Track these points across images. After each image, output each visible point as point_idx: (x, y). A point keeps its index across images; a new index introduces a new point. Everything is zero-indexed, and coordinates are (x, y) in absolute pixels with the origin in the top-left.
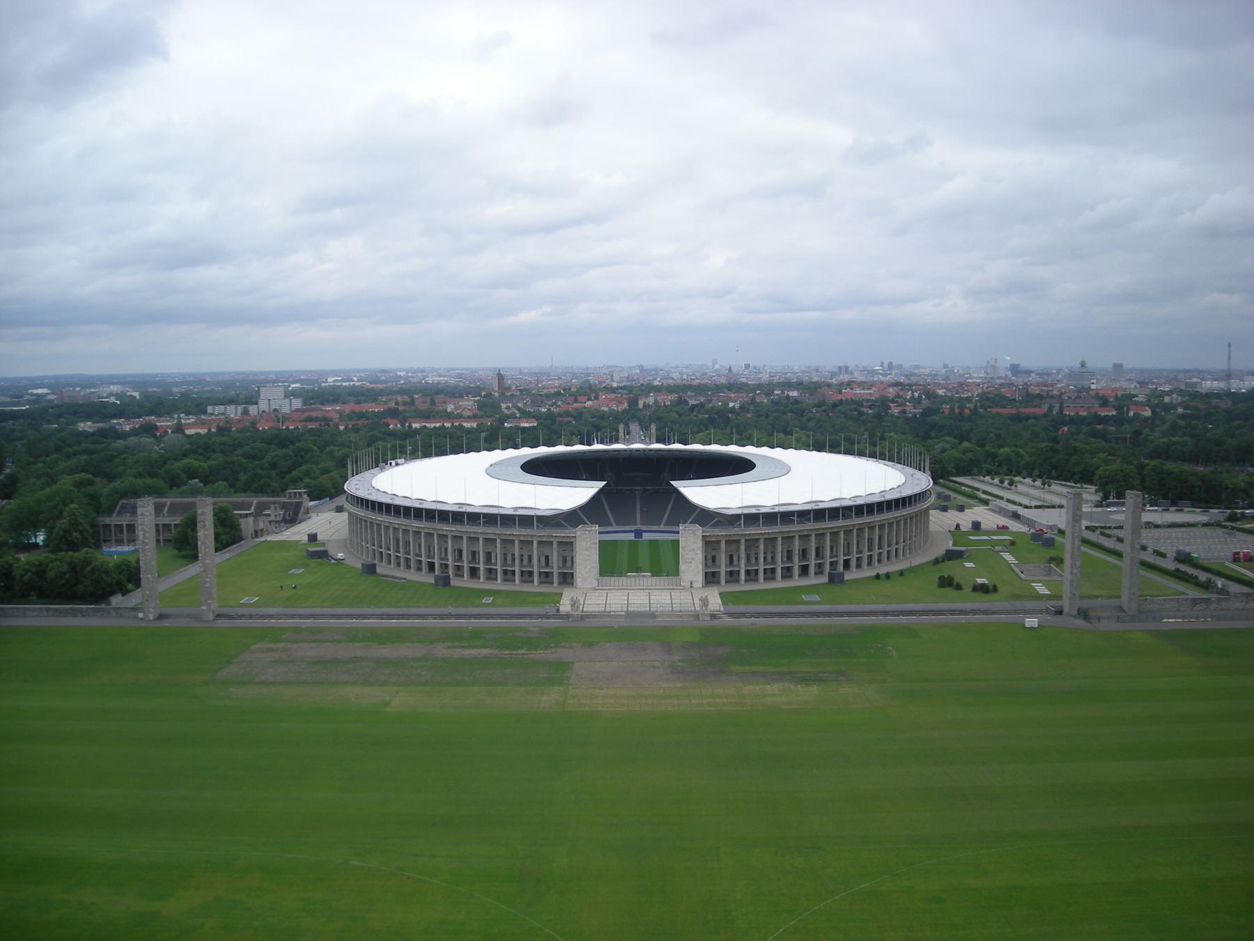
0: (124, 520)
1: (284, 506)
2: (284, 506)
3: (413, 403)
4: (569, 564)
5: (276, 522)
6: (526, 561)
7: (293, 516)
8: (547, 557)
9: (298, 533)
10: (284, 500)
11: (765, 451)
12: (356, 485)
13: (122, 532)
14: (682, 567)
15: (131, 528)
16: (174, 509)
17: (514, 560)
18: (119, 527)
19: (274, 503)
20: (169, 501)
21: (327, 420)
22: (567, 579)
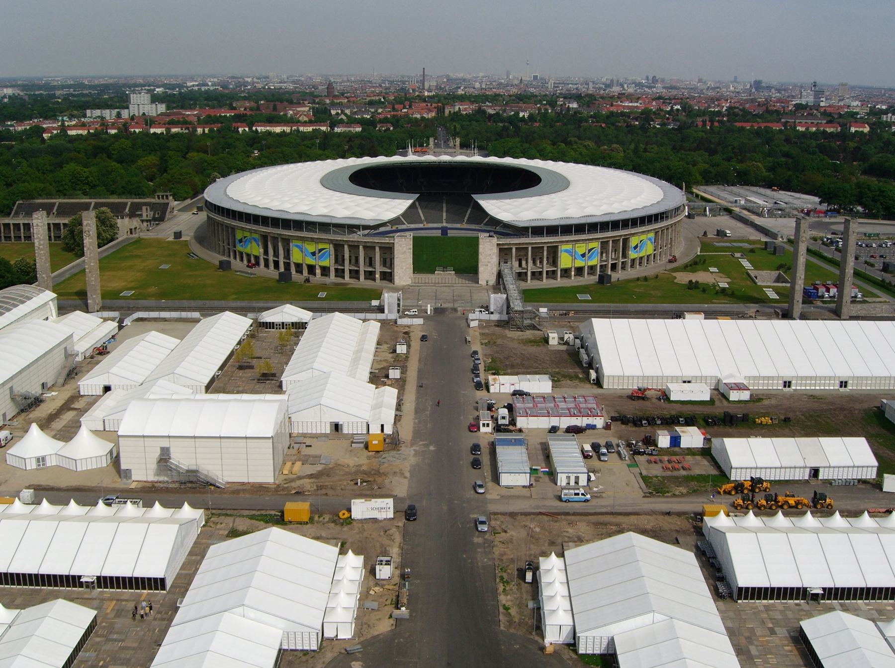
0: (21, 221)
1: (153, 207)
2: (153, 207)
3: (258, 108)
4: (388, 264)
5: (147, 221)
6: (353, 261)
7: (160, 215)
8: (371, 259)
9: (165, 232)
10: (153, 200)
11: (549, 165)
12: (213, 193)
13: (19, 230)
14: (481, 269)
15: (28, 226)
16: (63, 211)
17: (343, 260)
18: (17, 226)
19: (146, 204)
20: (57, 201)
21: (185, 123)
22: (388, 277)
